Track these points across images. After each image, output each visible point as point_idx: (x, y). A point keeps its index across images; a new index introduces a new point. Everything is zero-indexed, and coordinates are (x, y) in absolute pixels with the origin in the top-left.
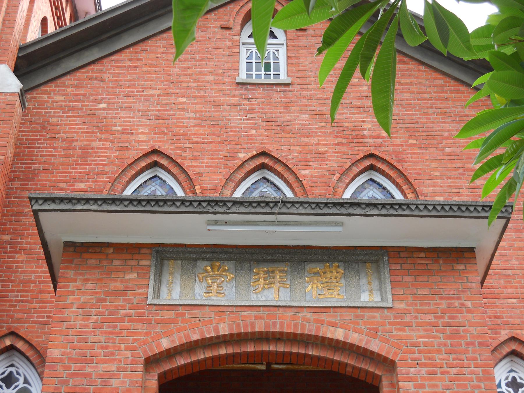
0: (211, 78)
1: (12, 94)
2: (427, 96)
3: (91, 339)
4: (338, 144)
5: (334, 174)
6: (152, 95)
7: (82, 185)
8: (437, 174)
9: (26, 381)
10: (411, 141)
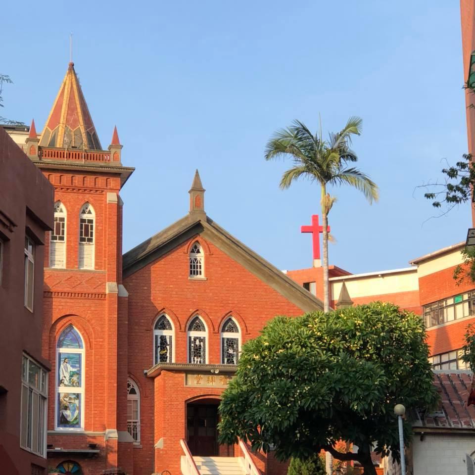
0: (180, 277)
1: (126, 297)
2: (250, 286)
3: (173, 396)
4: (220, 306)
5: (219, 318)
6: (162, 284)
7: (143, 321)
8: (251, 319)
9: (133, 386)
10: (244, 306)
